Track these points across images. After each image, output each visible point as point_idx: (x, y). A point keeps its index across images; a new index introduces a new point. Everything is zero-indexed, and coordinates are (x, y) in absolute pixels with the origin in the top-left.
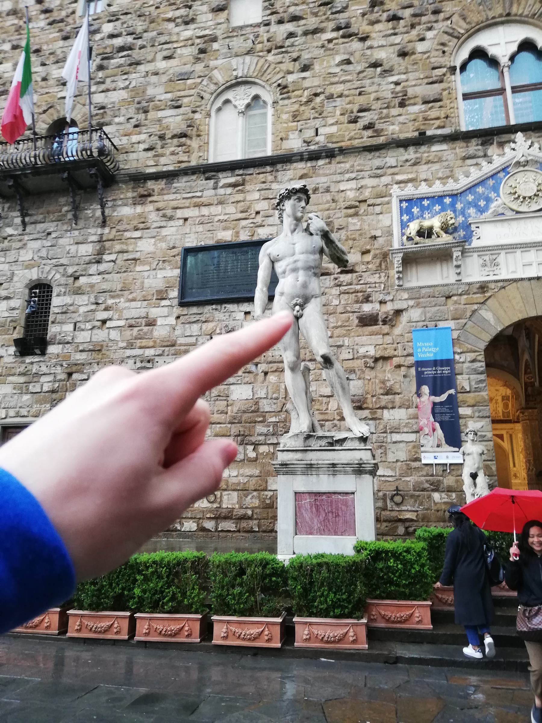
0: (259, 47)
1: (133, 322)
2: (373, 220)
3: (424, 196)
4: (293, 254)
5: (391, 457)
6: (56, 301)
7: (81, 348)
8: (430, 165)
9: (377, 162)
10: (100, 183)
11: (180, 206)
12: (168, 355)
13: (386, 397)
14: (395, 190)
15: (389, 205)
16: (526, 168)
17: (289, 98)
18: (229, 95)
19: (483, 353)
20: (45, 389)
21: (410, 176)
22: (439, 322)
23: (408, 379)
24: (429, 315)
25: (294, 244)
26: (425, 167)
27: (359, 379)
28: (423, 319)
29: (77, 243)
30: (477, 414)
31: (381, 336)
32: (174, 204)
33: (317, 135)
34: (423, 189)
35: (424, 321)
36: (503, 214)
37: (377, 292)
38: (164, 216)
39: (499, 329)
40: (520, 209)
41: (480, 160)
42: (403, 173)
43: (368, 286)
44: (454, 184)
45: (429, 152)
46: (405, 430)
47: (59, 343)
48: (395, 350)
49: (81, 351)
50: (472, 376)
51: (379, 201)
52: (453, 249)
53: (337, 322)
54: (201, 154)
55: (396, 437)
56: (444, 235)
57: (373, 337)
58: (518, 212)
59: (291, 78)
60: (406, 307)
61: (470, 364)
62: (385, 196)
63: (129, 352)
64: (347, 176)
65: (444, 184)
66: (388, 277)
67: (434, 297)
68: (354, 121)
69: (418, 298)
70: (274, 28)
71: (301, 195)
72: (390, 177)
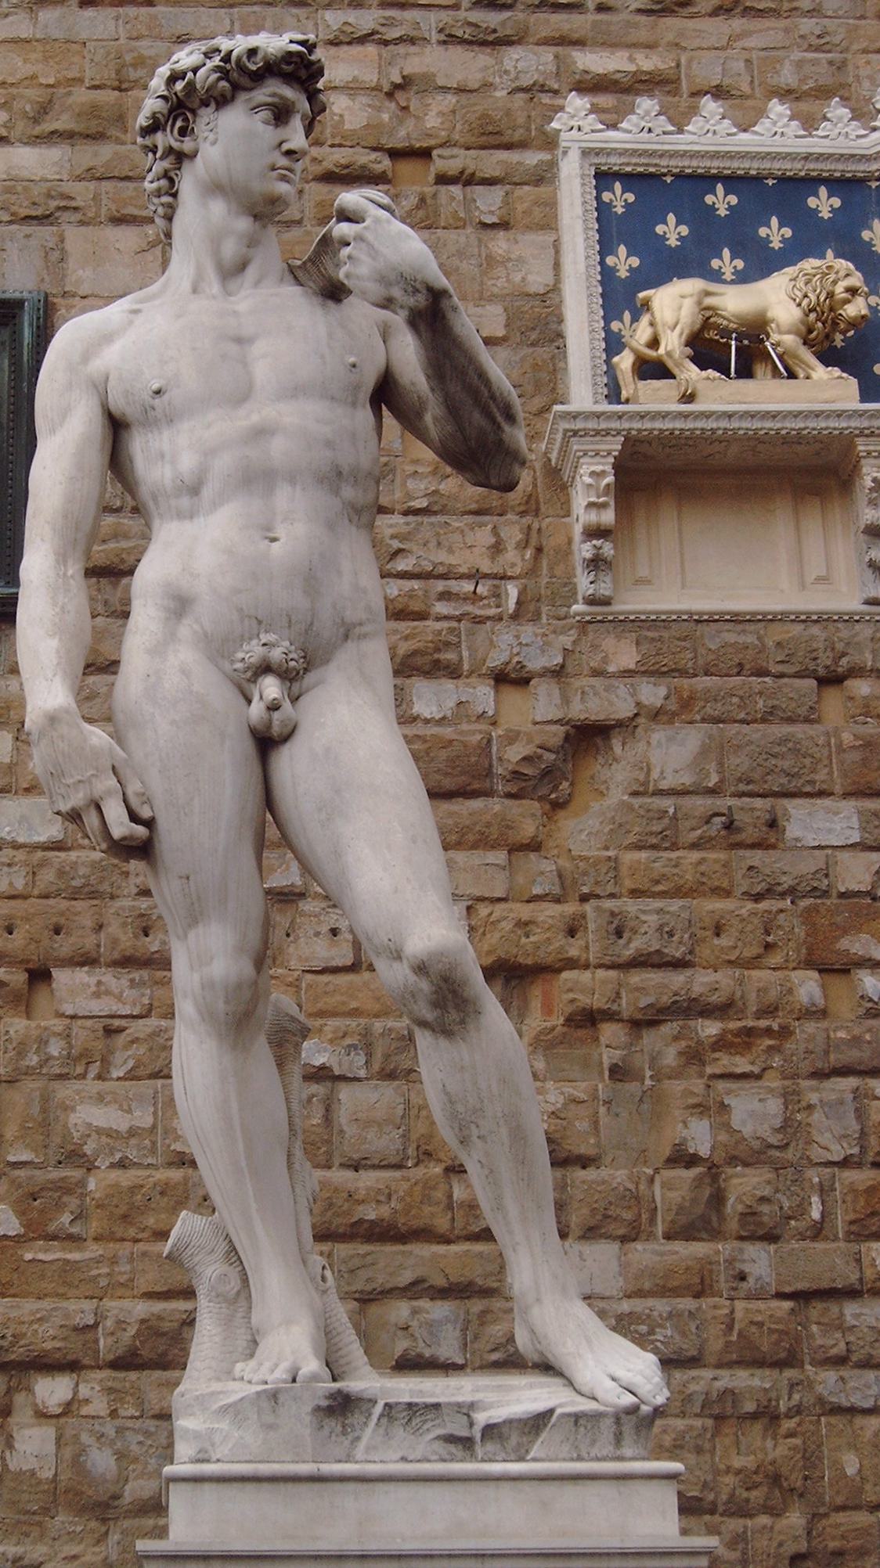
3: (715, 166)
4: (243, 395)
14: (576, 120)
15: (543, 190)
21: (647, 62)
22: (785, 802)
23: (633, 1087)
24: (739, 762)
25: (239, 340)
28: (713, 780)
31: (500, 857)
34: (710, 134)
35: (712, 792)
37: (479, 621)
42: (611, 44)
43: (440, 586)
48: (572, 932)
51: (492, 162)
60: (623, 708)
62: (522, 145)
66: (539, 550)
67: (761, 673)
69: (683, 673)
71: (289, 92)
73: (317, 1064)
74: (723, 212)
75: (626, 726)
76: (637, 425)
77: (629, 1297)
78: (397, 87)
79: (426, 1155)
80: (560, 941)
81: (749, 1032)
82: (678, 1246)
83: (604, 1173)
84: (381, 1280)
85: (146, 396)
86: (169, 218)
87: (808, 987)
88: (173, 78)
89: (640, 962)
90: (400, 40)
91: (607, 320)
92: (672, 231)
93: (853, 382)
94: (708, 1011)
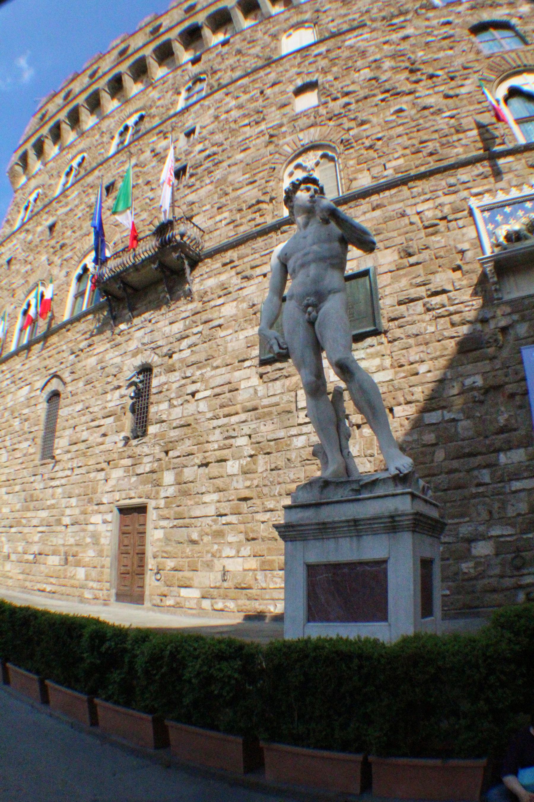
0: (320, 119)
1: (217, 390)
2: (457, 235)
5: (511, 512)
6: (155, 382)
7: (174, 425)
10: (186, 262)
11: (259, 263)
12: (252, 420)
13: (502, 436)
17: (352, 147)
18: (300, 160)
20: (148, 469)
23: (524, 410)
27: (468, 418)
29: (170, 324)
31: (488, 362)
32: (253, 263)
33: (385, 169)
38: (243, 278)
42: (478, 186)
46: (525, 474)
47: (156, 423)
49: (174, 428)
53: (435, 352)
54: (275, 213)
55: (517, 485)
57: (479, 364)
59: (352, 133)
63: (215, 423)
64: (422, 198)
66: (485, 291)
68: (418, 152)
70: (331, 104)
73: (452, 417)
77: (528, 460)
79: (479, 434)
80: (503, 378)
83: (519, 432)
84: (471, 466)
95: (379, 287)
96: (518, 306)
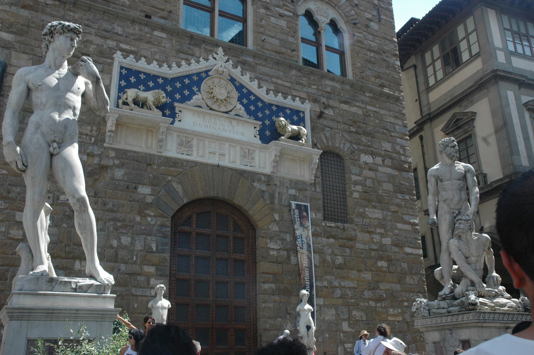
3: (142, 70)
8: (150, 46)
9: (106, 25)
14: (118, 56)
16: (221, 76)
19: (170, 219)
23: (103, 233)
26: (146, 46)
30: (159, 273)
35: (126, 181)
36: (200, 107)
39: (185, 201)
40: (214, 107)
41: (189, 57)
42: (127, 44)
44: (168, 69)
45: (151, 34)
50: (159, 238)
52: (161, 124)
56: (155, 109)
58: (211, 109)
61: (159, 228)
62: (108, 58)
65: (160, 66)
67: (137, 161)
72: (115, 43)
74: (142, 78)
75: (111, 167)
76: (121, 113)
78: (85, 41)
79: (61, 242)
81: (126, 225)
82: (108, 263)
85: (37, 85)
86: (46, 53)
87: (138, 219)
88: (52, 26)
89: (108, 210)
90: (87, 33)
91: (119, 93)
92: (133, 80)
93: (161, 113)
94: (119, 221)
95: (4, 84)
96: (121, 154)
